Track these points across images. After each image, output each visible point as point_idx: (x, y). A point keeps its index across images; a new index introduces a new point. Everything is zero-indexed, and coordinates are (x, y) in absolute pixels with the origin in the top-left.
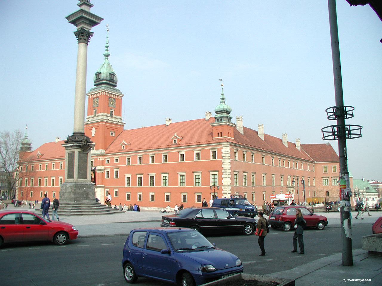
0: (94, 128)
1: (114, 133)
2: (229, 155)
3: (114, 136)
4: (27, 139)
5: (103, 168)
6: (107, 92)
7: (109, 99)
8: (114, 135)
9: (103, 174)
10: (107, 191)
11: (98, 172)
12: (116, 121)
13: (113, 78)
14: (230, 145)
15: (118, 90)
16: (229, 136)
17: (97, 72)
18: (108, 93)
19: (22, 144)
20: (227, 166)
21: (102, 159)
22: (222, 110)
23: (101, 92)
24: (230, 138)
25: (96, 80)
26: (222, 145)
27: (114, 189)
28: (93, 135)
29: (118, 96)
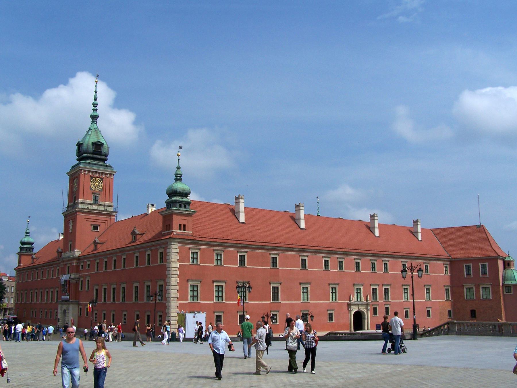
1: (99, 228)
2: (178, 257)
4: (29, 236)
5: (77, 276)
7: (91, 179)
9: (77, 284)
10: (81, 309)
11: (71, 282)
12: (101, 209)
13: (100, 149)
14: (179, 243)
15: (106, 166)
16: (180, 229)
18: (89, 172)
19: (23, 243)
20: (175, 272)
22: (171, 192)
24: (184, 231)
25: (78, 153)
26: (167, 243)
28: (70, 231)
29: (106, 174)
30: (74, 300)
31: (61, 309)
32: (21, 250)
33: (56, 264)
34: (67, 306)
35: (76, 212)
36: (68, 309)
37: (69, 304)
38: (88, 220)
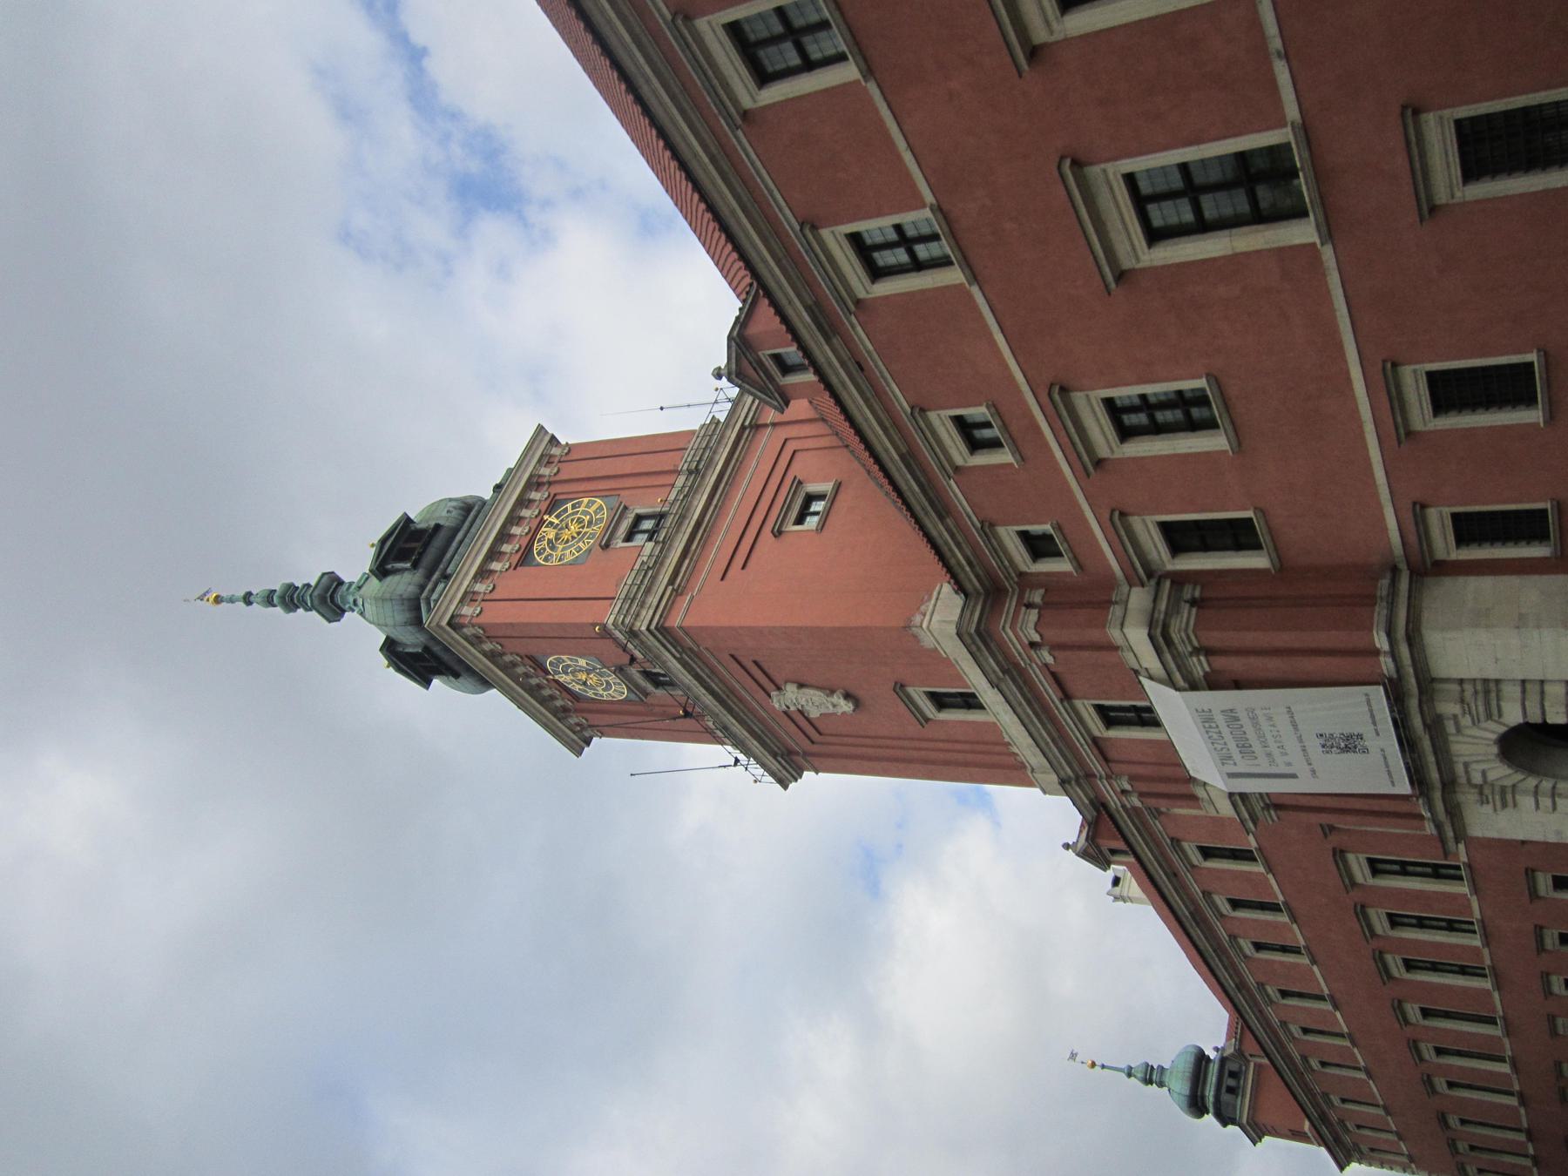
0: (778, 702)
3: (838, 487)
5: (1139, 598)
6: (466, 583)
8: (826, 487)
9: (1211, 596)
10: (1469, 528)
11: (1199, 666)
13: (423, 531)
17: (399, 670)
18: (483, 573)
21: (1033, 615)
23: (476, 641)
25: (457, 675)
27: (1400, 435)
28: (846, 707)
29: (534, 483)
30: (1380, 613)
31: (1505, 797)
32: (1233, 1121)
33: (1174, 875)
34: (1448, 708)
35: (663, 631)
36: (1489, 688)
37: (1428, 684)
38: (743, 555)
